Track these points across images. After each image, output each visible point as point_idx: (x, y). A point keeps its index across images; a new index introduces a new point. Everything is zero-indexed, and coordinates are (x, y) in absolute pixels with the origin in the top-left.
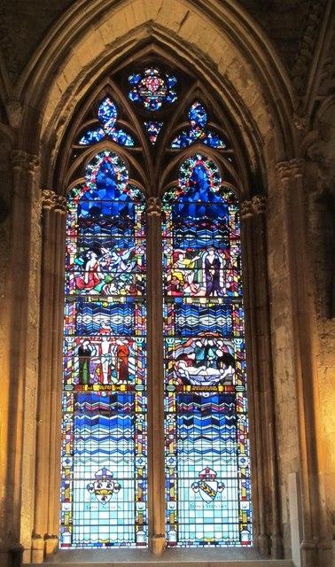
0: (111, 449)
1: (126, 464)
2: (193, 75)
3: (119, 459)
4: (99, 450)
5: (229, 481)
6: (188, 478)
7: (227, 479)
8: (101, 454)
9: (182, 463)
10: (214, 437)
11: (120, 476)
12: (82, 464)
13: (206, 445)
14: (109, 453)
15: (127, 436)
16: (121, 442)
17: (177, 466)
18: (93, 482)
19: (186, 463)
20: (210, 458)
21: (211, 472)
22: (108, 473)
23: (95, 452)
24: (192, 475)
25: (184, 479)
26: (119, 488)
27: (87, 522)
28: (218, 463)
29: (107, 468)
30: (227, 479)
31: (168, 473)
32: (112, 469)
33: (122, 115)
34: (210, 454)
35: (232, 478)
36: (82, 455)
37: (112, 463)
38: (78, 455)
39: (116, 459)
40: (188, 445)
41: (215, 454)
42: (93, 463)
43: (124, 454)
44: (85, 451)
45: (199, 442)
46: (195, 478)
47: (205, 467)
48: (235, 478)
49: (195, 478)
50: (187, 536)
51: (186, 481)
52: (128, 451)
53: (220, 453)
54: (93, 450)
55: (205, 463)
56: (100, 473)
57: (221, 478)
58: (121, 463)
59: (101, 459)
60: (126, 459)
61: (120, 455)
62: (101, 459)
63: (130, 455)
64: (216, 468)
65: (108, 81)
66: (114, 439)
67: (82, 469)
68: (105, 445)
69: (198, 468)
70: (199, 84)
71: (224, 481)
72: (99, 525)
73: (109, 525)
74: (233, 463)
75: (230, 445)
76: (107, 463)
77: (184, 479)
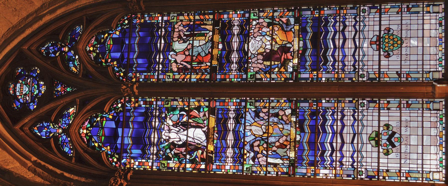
0: (352, 132)
1: (365, 118)
2: (16, 53)
3: (360, 124)
7: (380, 25)
8: (355, 141)
11: (376, 123)
12: (364, 160)
13: (350, 44)
15: (339, 117)
18: (381, 150)
19: (366, 63)
20: (361, 40)
21: (375, 39)
22: (374, 135)
23: (353, 147)
26: (387, 126)
28: (366, 33)
29: (368, 135)
30: (380, 25)
32: (370, 132)
33: (47, 117)
35: (380, 21)
36: (356, 159)
37: (364, 132)
38: (356, 164)
40: (349, 62)
42: (364, 149)
44: (352, 157)
47: (369, 46)
54: (351, 149)
55: (365, 45)
56: (373, 142)
57: (380, 31)
58: (365, 123)
59: (360, 142)
60: (360, 117)
61: (356, 124)
62: (360, 142)
64: (371, 36)
65: (17, 127)
68: (348, 139)
69: (371, 51)
70: (25, 47)
71: (383, 28)
72: (423, 145)
73: (423, 135)
74: (367, 19)
76: (365, 137)
77: (379, 65)
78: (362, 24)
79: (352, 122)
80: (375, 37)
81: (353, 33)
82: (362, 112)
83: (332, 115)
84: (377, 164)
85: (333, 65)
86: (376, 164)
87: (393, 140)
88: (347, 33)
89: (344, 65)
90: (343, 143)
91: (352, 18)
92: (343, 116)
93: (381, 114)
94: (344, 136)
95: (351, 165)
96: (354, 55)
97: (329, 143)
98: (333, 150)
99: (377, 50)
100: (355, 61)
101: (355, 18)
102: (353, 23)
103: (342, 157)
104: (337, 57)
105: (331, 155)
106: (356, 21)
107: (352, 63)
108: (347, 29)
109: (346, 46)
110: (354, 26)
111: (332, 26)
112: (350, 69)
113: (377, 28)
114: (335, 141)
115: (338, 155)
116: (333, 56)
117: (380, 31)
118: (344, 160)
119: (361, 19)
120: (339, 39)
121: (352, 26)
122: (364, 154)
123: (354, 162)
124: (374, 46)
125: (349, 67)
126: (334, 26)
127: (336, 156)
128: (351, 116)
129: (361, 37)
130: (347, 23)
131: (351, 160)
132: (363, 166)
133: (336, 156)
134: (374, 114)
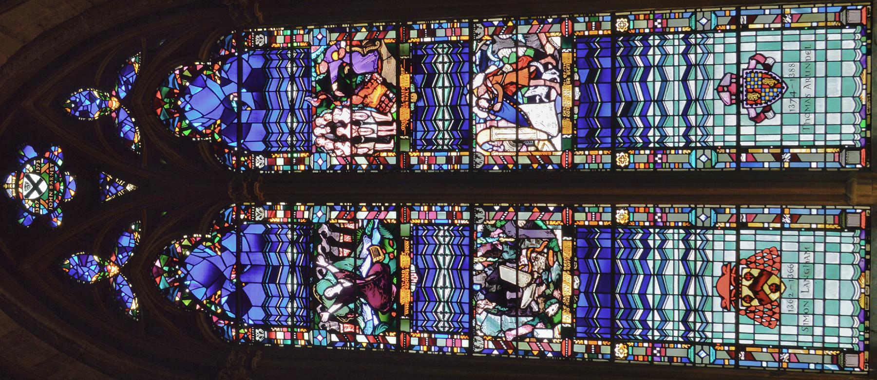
4: (684, 294)
5: (744, 47)
6: (738, 126)
7: (738, 52)
8: (691, 291)
9: (711, 139)
10: (658, 77)
12: (709, 328)
13: (675, 91)
14: (688, 276)
16: (669, 254)
17: (714, 148)
21: (726, 82)
24: (731, 120)
25: (738, 134)
27: (819, 320)
30: (738, 52)
31: (724, 163)
34: (692, 84)
35: (738, 44)
38: (691, 335)
39: (699, 264)
41: (692, 75)
42: (708, 307)
43: (691, 249)
45: (669, 106)
46: (738, 114)
47: (717, 97)
48: (738, 37)
49: (738, 114)
50: (851, 129)
51: (743, 131)
52: (685, 240)
53: (689, 66)
54: (682, 306)
55: (709, 95)
57: (738, 63)
58: (709, 253)
59: (699, 292)
60: (699, 243)
63: (693, 237)
64: (719, 74)
66: (662, 267)
67: (718, 328)
69: (719, 107)
74: (711, 41)
75: (674, 46)
76: (708, 280)
78: (699, 51)
79: (682, 252)
80: (728, 77)
81: (683, 69)
82: (704, 234)
83: (644, 241)
84: (734, 334)
85: (644, 136)
86: (733, 336)
87: (766, 288)
88: (669, 72)
89: (664, 136)
90: (664, 295)
91: (679, 39)
92: (664, 241)
93: (742, 237)
94: (668, 281)
95: (682, 337)
96: (685, 114)
97: (639, 294)
98: (647, 309)
99: (732, 104)
100: (689, 127)
101: (685, 39)
102: (682, 48)
103: (664, 320)
104: (651, 119)
105: (643, 321)
106: (689, 46)
107: (682, 130)
108: (669, 60)
109: (668, 96)
110: (685, 54)
111: (640, 55)
112: (679, 142)
113: (732, 58)
114: (650, 290)
115: (657, 317)
116: (643, 116)
117: (738, 63)
118: (669, 326)
119: (698, 41)
120: (654, 81)
121: (679, 54)
122: (709, 315)
123: (688, 330)
124: (726, 96)
125: (676, 139)
126: (644, 55)
127: (653, 320)
128: (681, 242)
129: (700, 77)
130: (670, 50)
131: (682, 327)
132: (706, 338)
133: (653, 320)
134: (728, 238)
